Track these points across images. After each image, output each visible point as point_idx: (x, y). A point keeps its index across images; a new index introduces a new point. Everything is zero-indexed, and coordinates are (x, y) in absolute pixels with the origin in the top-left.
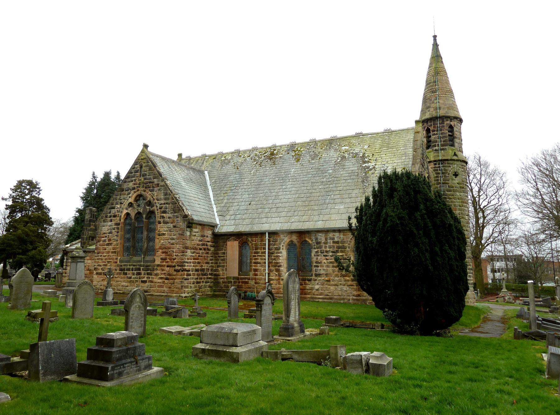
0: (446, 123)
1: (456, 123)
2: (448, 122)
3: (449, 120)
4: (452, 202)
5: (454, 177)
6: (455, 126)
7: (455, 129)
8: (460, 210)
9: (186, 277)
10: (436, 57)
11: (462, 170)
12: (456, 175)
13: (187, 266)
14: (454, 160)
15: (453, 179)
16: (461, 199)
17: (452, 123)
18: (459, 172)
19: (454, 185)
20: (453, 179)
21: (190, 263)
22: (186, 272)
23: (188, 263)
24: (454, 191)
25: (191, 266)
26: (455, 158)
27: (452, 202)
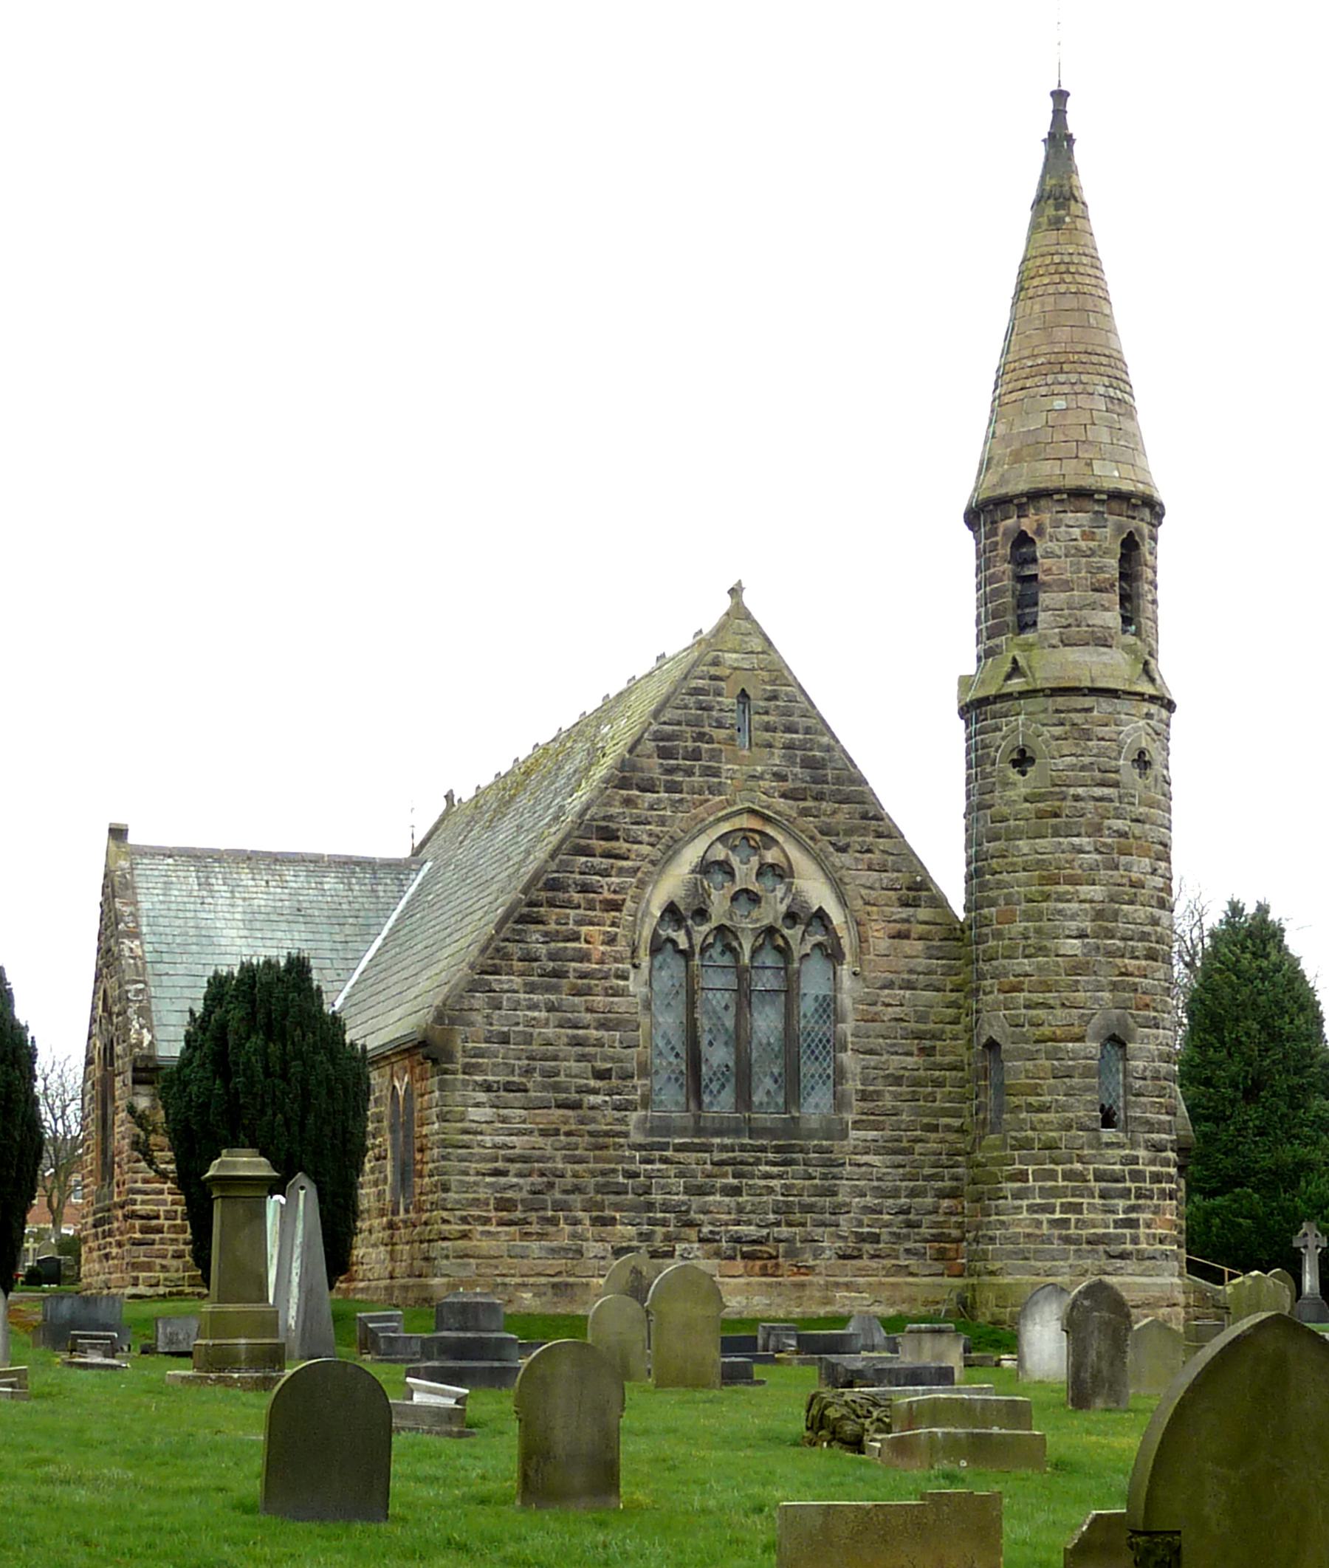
0: (1002, 526)
1: (1046, 518)
2: (1009, 522)
3: (1013, 509)
4: (999, 885)
5: (1013, 774)
6: (1040, 531)
7: (1041, 547)
8: (1028, 917)
9: (138, 1235)
10: (1058, 200)
11: (1058, 731)
12: (1022, 760)
13: (143, 1202)
14: (1009, 696)
15: (1006, 784)
16: (1040, 864)
17: (1027, 525)
18: (1039, 746)
19: (1006, 810)
20: (1006, 784)
21: (161, 1192)
22: (138, 1223)
23: (146, 1193)
24: (1012, 836)
25: (164, 1203)
26: (1016, 684)
27: (999, 885)
